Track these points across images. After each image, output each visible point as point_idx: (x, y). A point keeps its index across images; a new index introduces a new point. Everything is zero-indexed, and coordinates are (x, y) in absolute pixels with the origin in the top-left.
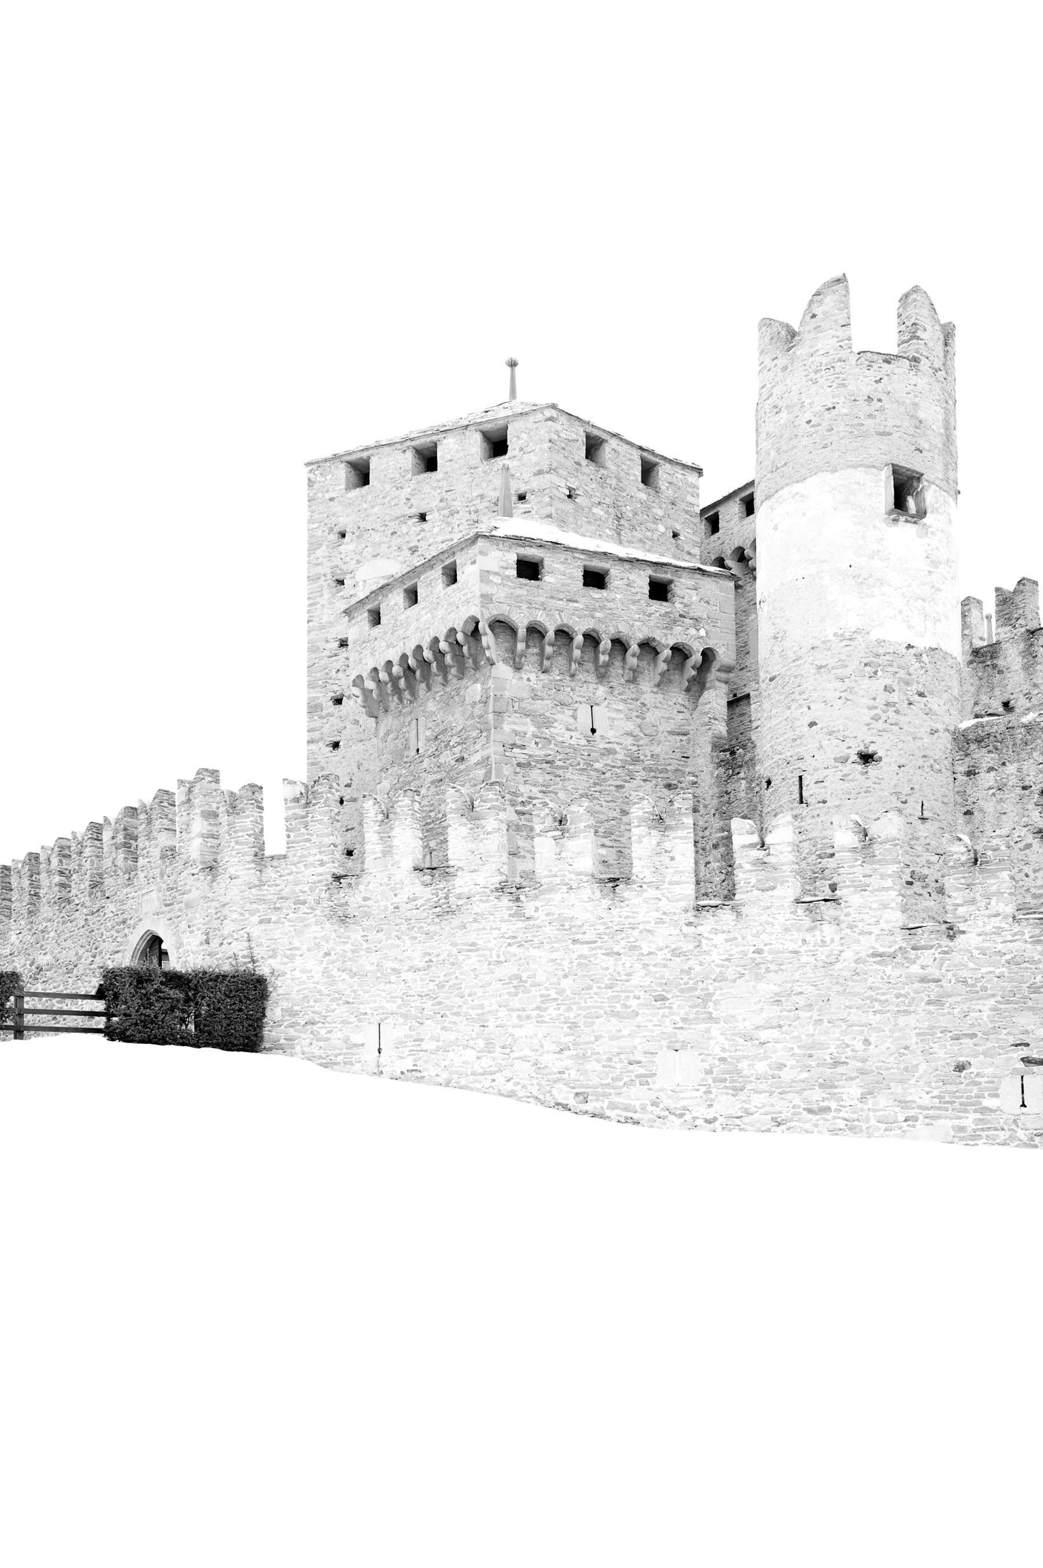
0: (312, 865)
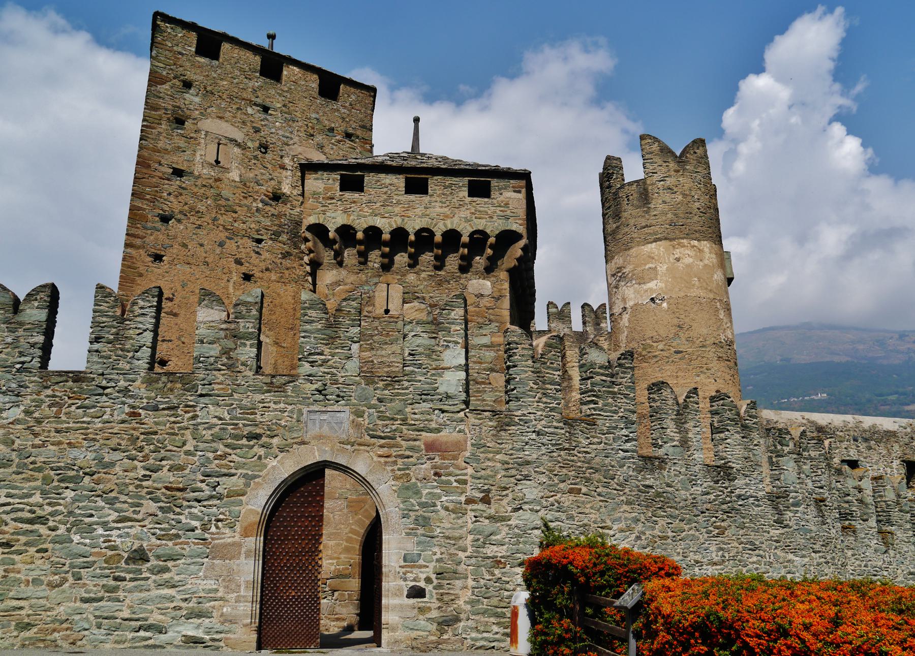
0: (619, 438)
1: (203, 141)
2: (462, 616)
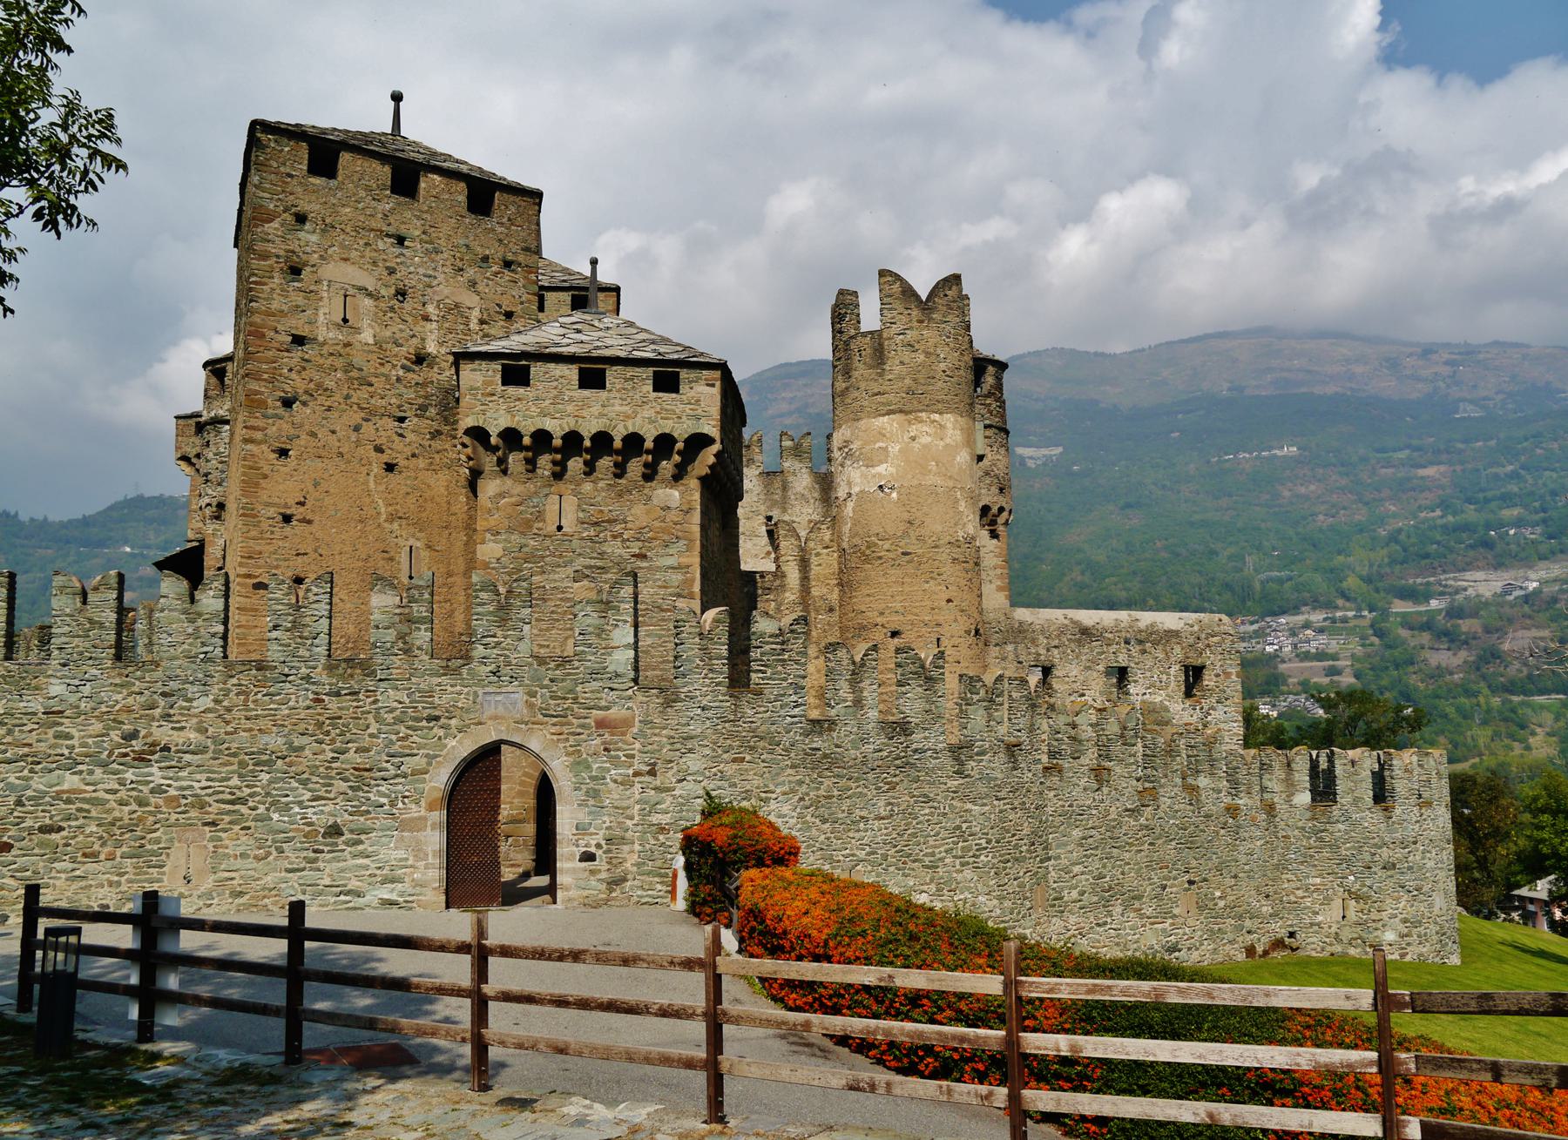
1: (325, 294)
2: (629, 877)
